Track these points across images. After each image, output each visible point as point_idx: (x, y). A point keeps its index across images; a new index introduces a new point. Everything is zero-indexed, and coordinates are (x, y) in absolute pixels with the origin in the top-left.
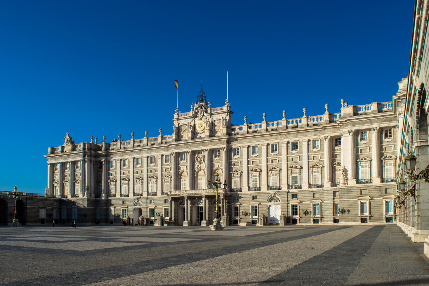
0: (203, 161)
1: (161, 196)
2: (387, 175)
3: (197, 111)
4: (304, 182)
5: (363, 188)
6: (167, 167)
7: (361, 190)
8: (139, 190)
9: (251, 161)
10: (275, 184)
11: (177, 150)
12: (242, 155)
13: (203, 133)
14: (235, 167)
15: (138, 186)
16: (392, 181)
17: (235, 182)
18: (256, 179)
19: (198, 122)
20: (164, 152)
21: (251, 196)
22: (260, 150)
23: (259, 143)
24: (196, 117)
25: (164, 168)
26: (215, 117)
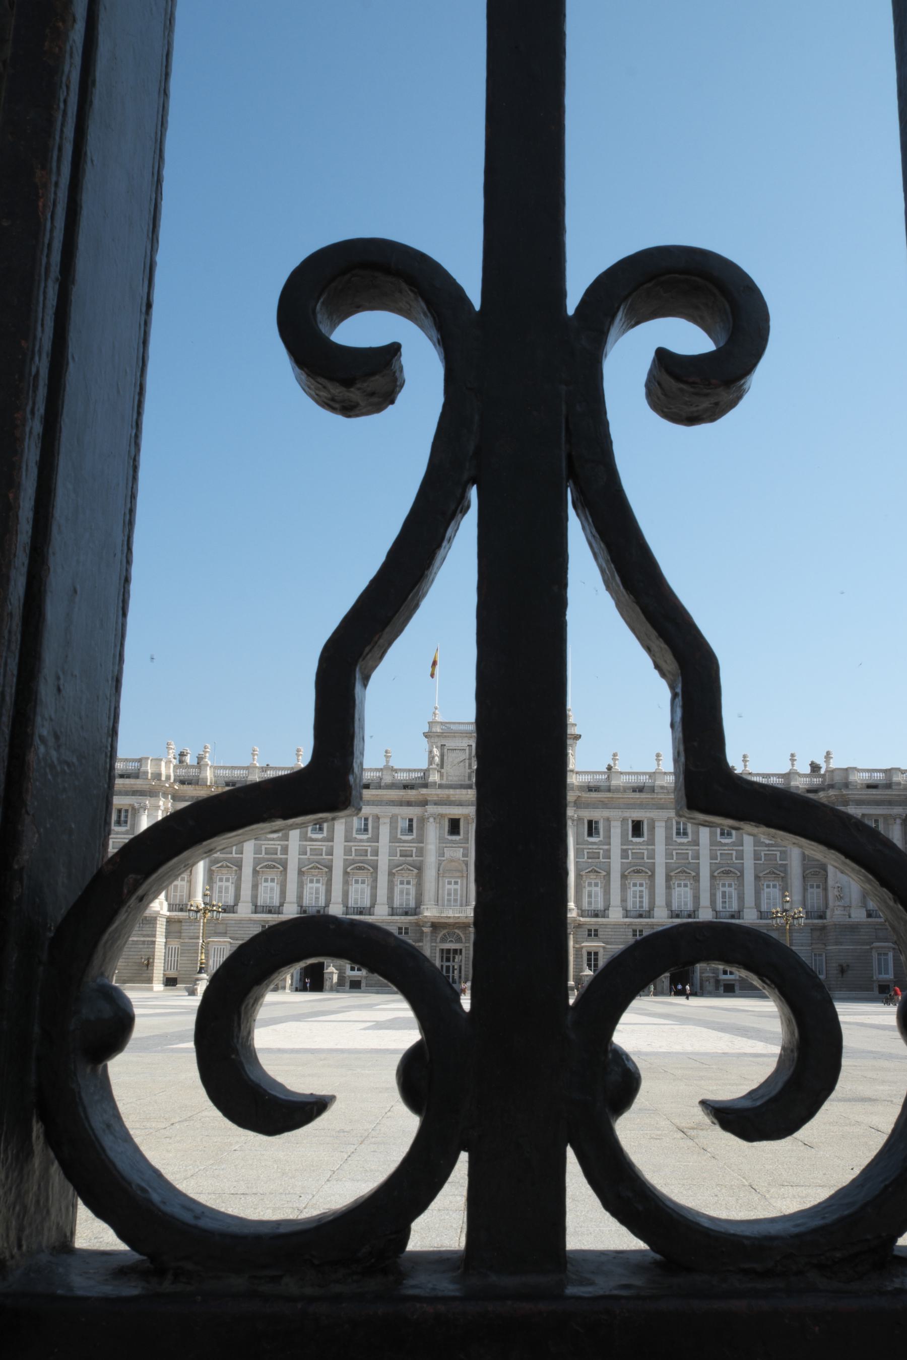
4: (746, 905)
5: (880, 927)
6: (406, 847)
7: (875, 929)
8: (317, 898)
10: (684, 905)
12: (609, 837)
14: (590, 860)
15: (311, 888)
17: (590, 896)
18: (641, 891)
21: (631, 930)
22: (652, 829)
25: (398, 849)
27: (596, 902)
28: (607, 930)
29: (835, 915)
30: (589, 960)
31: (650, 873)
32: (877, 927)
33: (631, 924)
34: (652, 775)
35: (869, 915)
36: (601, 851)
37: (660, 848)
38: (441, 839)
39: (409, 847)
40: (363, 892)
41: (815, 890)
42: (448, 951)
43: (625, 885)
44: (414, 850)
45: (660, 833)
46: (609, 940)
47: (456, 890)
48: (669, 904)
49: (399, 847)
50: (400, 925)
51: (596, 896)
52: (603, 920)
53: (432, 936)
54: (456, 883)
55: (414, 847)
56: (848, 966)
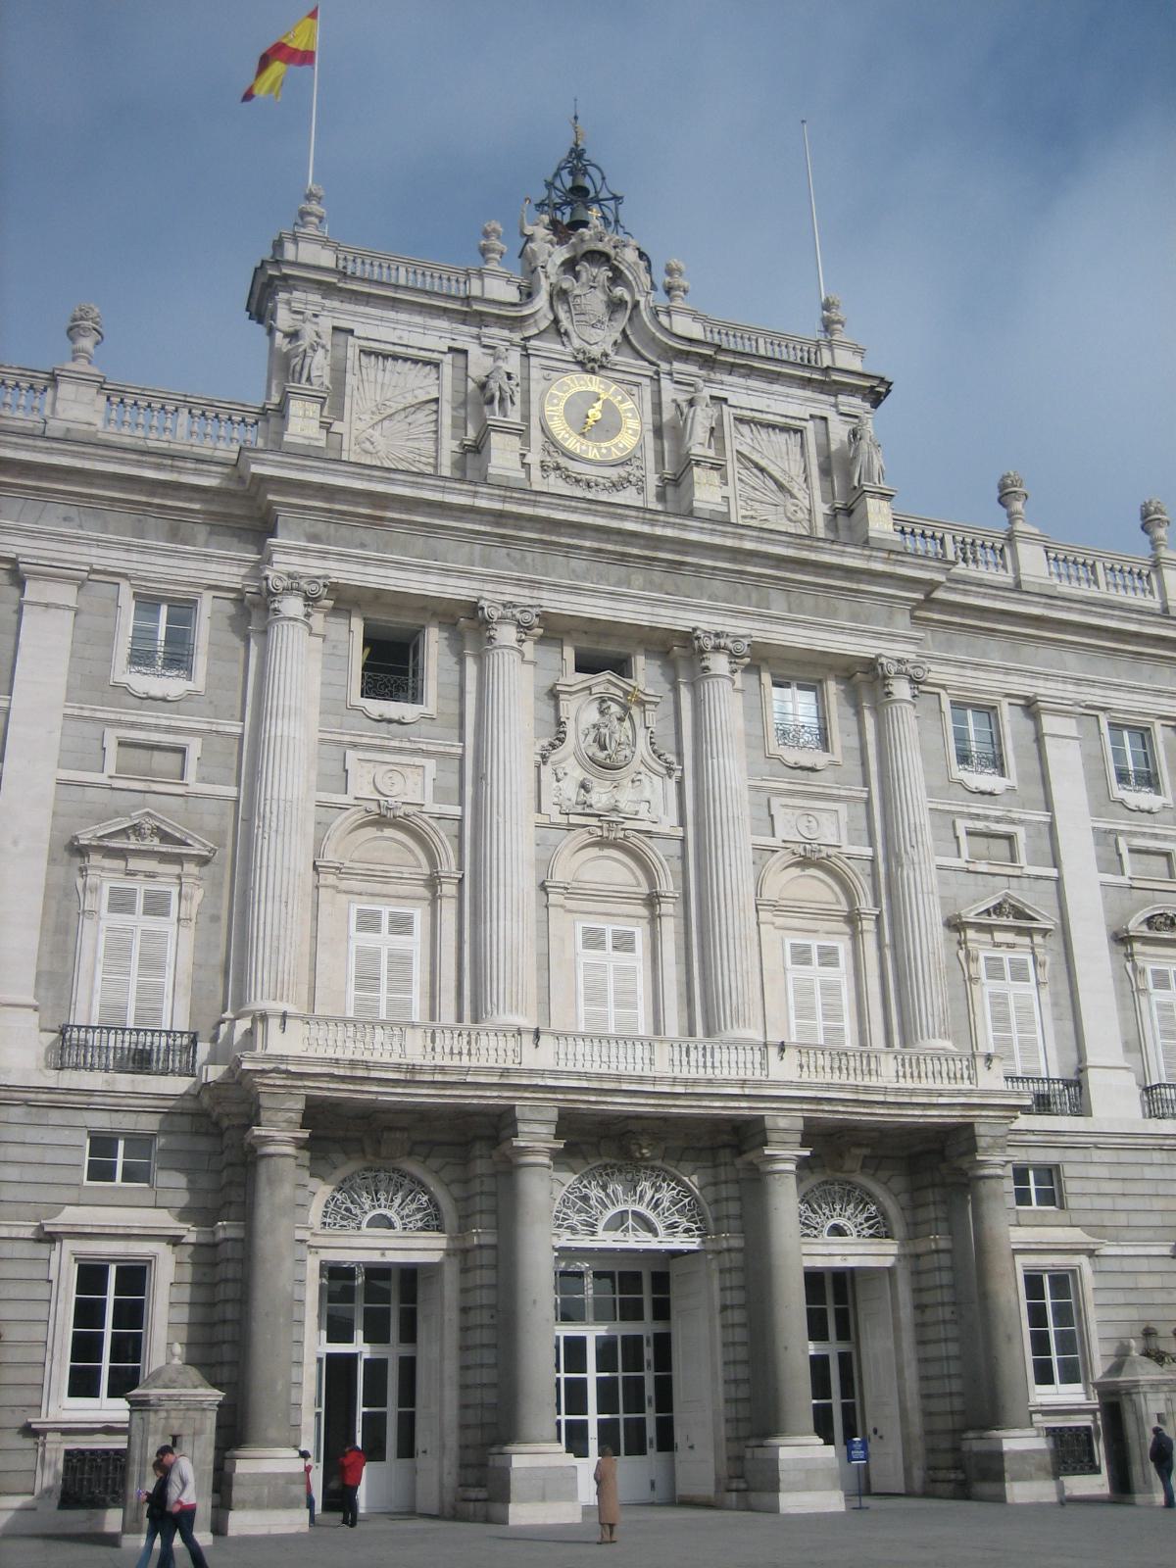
1: (51, 1079)
6: (154, 725)
11: (342, 557)
17: (1001, 1019)
20: (128, 548)
24: (556, 329)
25: (111, 736)
27: (1028, 1046)
28: (1094, 1171)
36: (1021, 833)
38: (331, 707)
39: (169, 730)
46: (1107, 1219)
47: (401, 961)
49: (119, 724)
50: (101, 1121)
51: (1024, 1010)
54: (402, 925)
55: (192, 732)
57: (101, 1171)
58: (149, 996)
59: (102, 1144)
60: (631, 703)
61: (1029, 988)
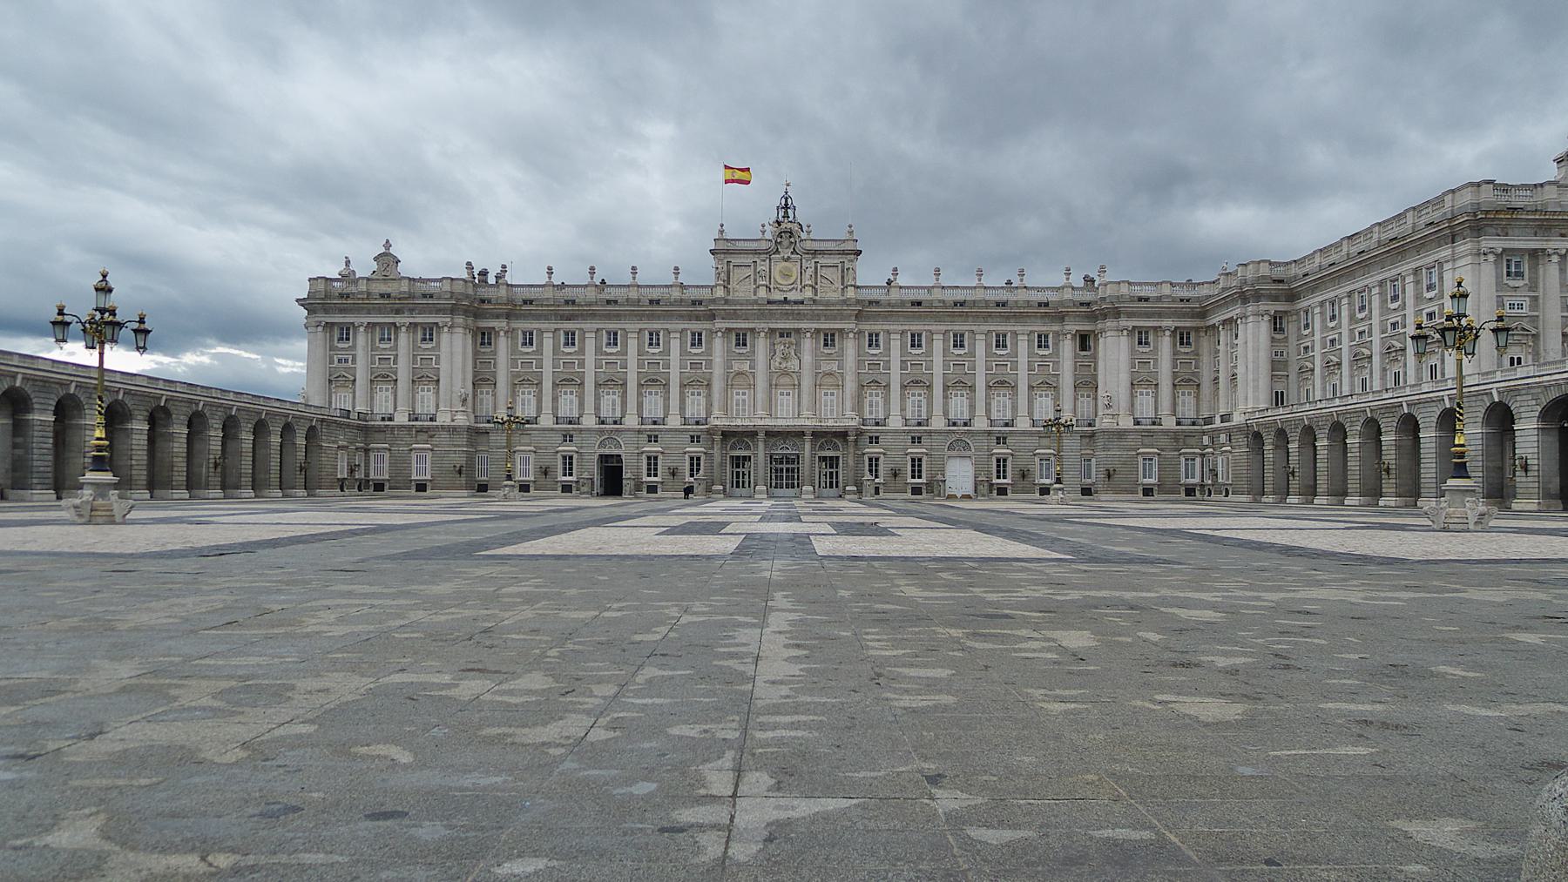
0: (793, 353)
1: (683, 427)
2: (1183, 413)
3: (779, 240)
5: (1146, 434)
8: (614, 410)
9: (909, 363)
10: (961, 413)
13: (791, 290)
14: (871, 372)
15: (608, 400)
16: (1194, 424)
17: (871, 406)
19: (778, 267)
23: (927, 328)
24: (777, 252)
25: (689, 362)
26: (823, 260)
27: (877, 412)
29: (1104, 423)
30: (870, 465)
31: (928, 384)
32: (1143, 434)
33: (910, 431)
34: (929, 289)
35: (1137, 423)
37: (938, 359)
40: (656, 404)
41: (1086, 399)
42: (738, 457)
43: (905, 395)
44: (704, 362)
45: (938, 345)
47: (744, 401)
48: (946, 413)
50: (692, 434)
51: (877, 403)
52: (884, 428)
53: (722, 444)
54: (744, 394)
56: (1114, 470)
57: (692, 441)
58: (699, 410)
59: (692, 437)
60: (791, 343)
61: (879, 399)
